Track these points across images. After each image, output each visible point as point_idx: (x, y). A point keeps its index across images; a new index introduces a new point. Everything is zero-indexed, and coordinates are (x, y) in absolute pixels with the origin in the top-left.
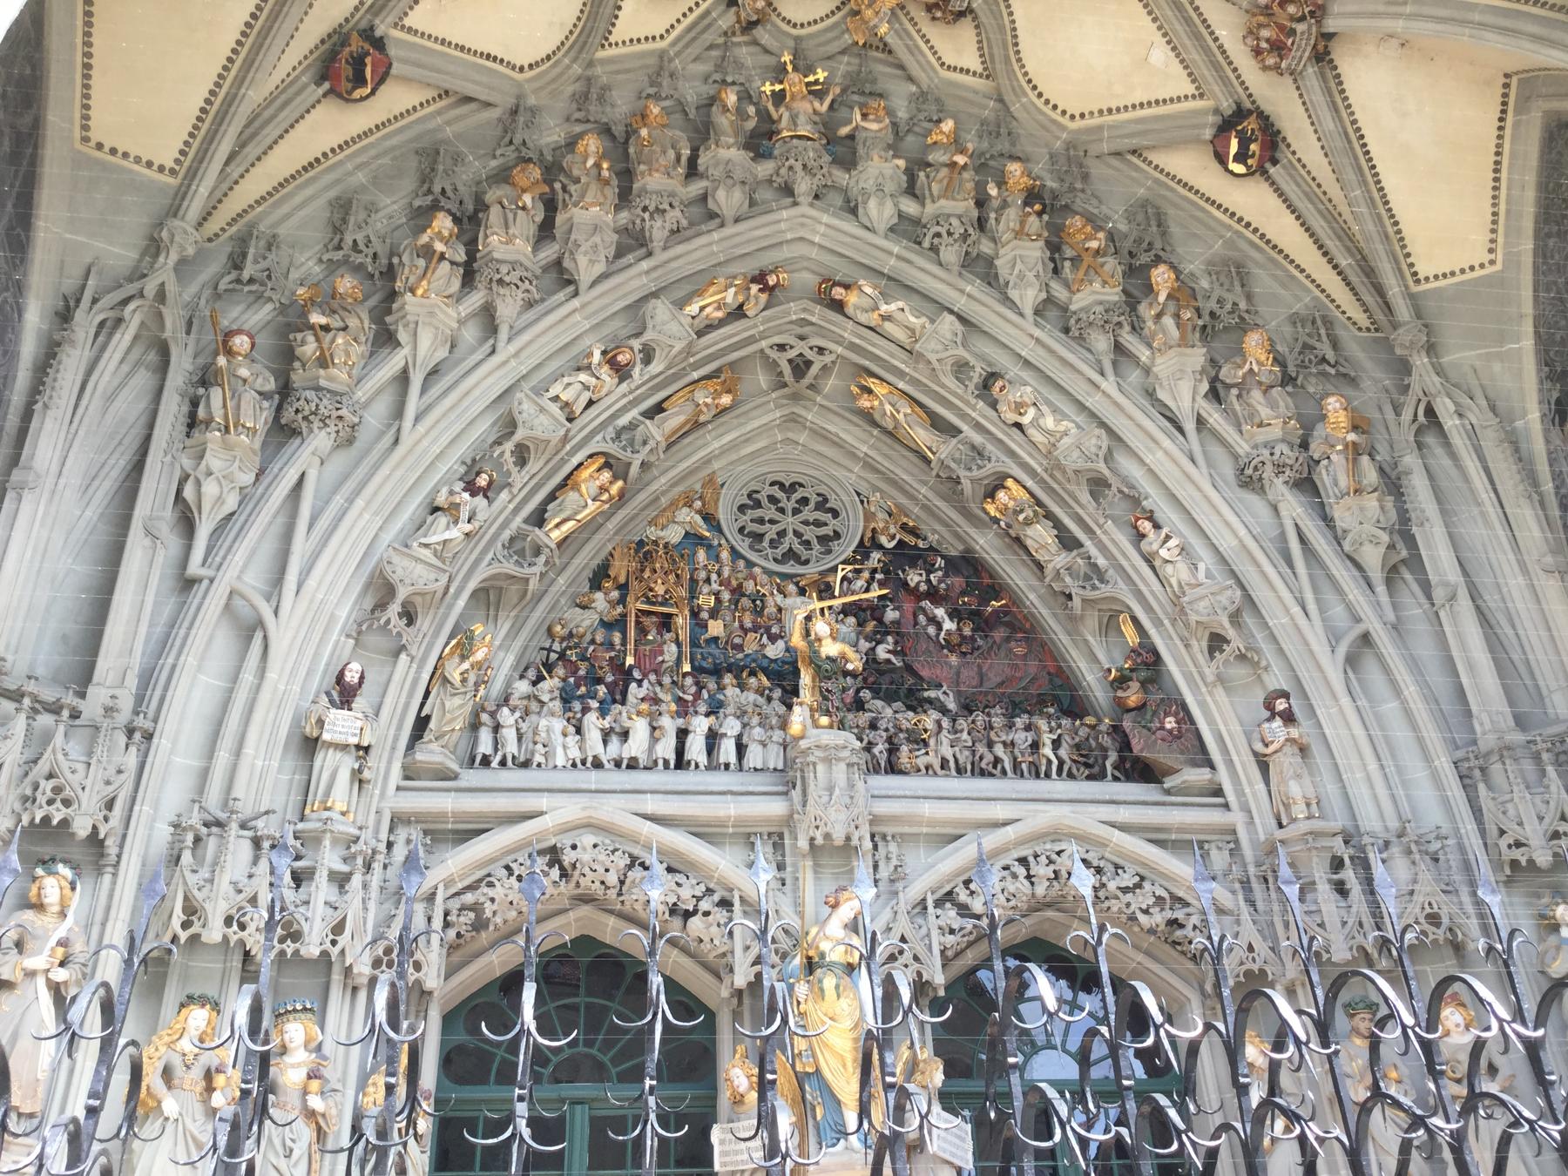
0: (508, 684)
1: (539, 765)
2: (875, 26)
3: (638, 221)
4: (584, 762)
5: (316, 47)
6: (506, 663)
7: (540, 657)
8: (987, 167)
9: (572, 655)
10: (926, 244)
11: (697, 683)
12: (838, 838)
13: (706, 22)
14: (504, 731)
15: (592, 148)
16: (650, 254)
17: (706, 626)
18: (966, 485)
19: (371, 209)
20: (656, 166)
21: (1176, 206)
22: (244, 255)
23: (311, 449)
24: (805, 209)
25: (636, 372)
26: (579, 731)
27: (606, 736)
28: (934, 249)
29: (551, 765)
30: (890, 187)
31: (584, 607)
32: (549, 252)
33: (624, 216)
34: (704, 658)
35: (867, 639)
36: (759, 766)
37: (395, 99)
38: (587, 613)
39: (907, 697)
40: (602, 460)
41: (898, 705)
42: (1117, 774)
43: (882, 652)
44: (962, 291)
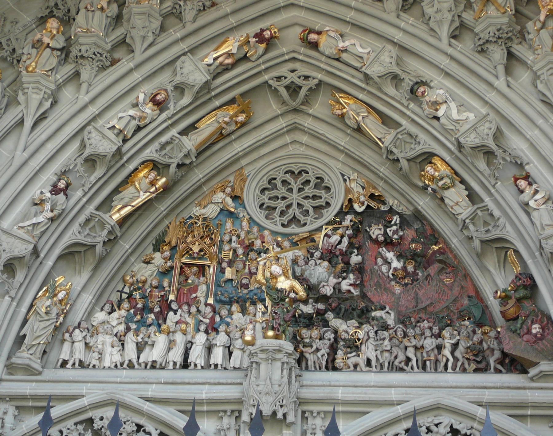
1: (94, 366)
4: (122, 364)
7: (115, 298)
9: (137, 295)
11: (214, 311)
12: (267, 411)
14: (75, 344)
17: (224, 273)
26: (123, 345)
27: (140, 347)
29: (102, 367)
31: (148, 263)
34: (222, 294)
35: (337, 276)
36: (237, 366)
38: (150, 266)
42: (499, 367)
43: (345, 286)
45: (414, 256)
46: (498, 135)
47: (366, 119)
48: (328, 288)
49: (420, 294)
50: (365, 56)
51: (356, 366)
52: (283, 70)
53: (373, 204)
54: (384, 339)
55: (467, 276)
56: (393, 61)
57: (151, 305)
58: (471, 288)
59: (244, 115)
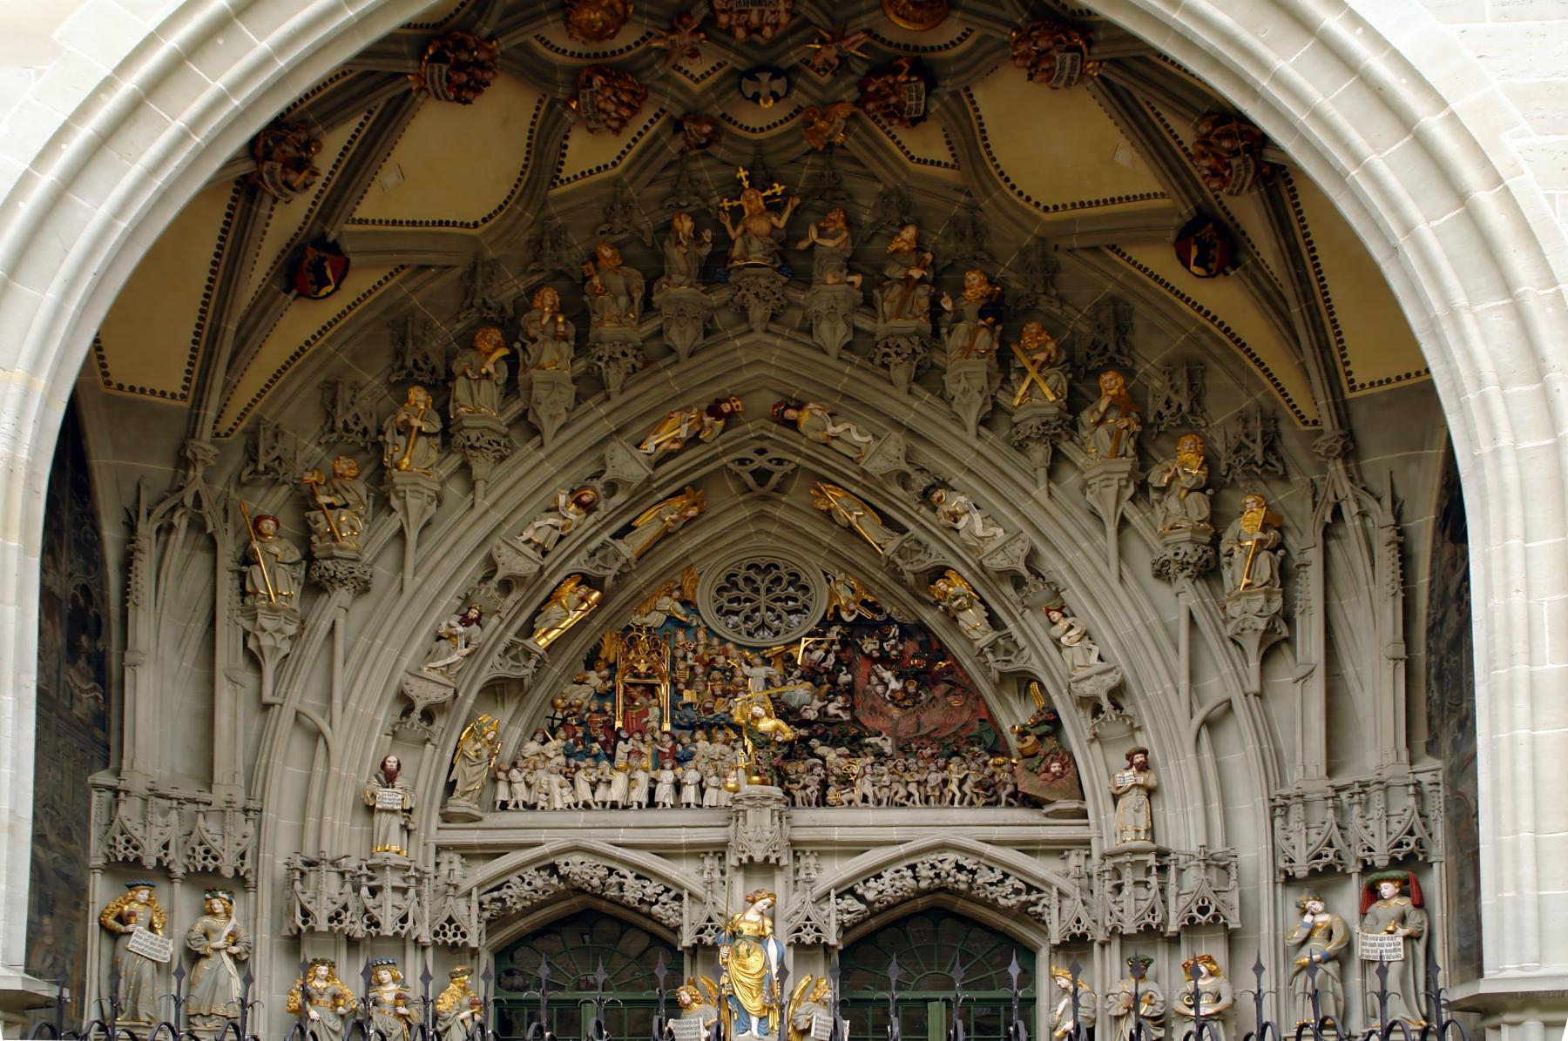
0: (520, 746)
2: (830, 137)
3: (596, 368)
5: (279, 257)
6: (516, 732)
8: (943, 278)
10: (877, 361)
13: (657, 145)
15: (549, 301)
16: (608, 398)
18: (910, 578)
19: (356, 388)
20: (607, 315)
21: (1146, 301)
22: (256, 448)
23: (336, 603)
24: (759, 336)
25: (601, 506)
28: (885, 366)
30: (843, 308)
32: (516, 407)
33: (581, 365)
37: (359, 283)
39: (850, 743)
40: (580, 578)
41: (843, 750)
44: (910, 407)
45: (917, 675)
46: (1032, 557)
47: (861, 519)
48: (811, 713)
49: (923, 718)
50: (863, 446)
51: (850, 802)
52: (747, 453)
53: (867, 614)
54: (882, 775)
55: (979, 697)
56: (902, 455)
57: (594, 734)
58: (983, 709)
59: (696, 508)
